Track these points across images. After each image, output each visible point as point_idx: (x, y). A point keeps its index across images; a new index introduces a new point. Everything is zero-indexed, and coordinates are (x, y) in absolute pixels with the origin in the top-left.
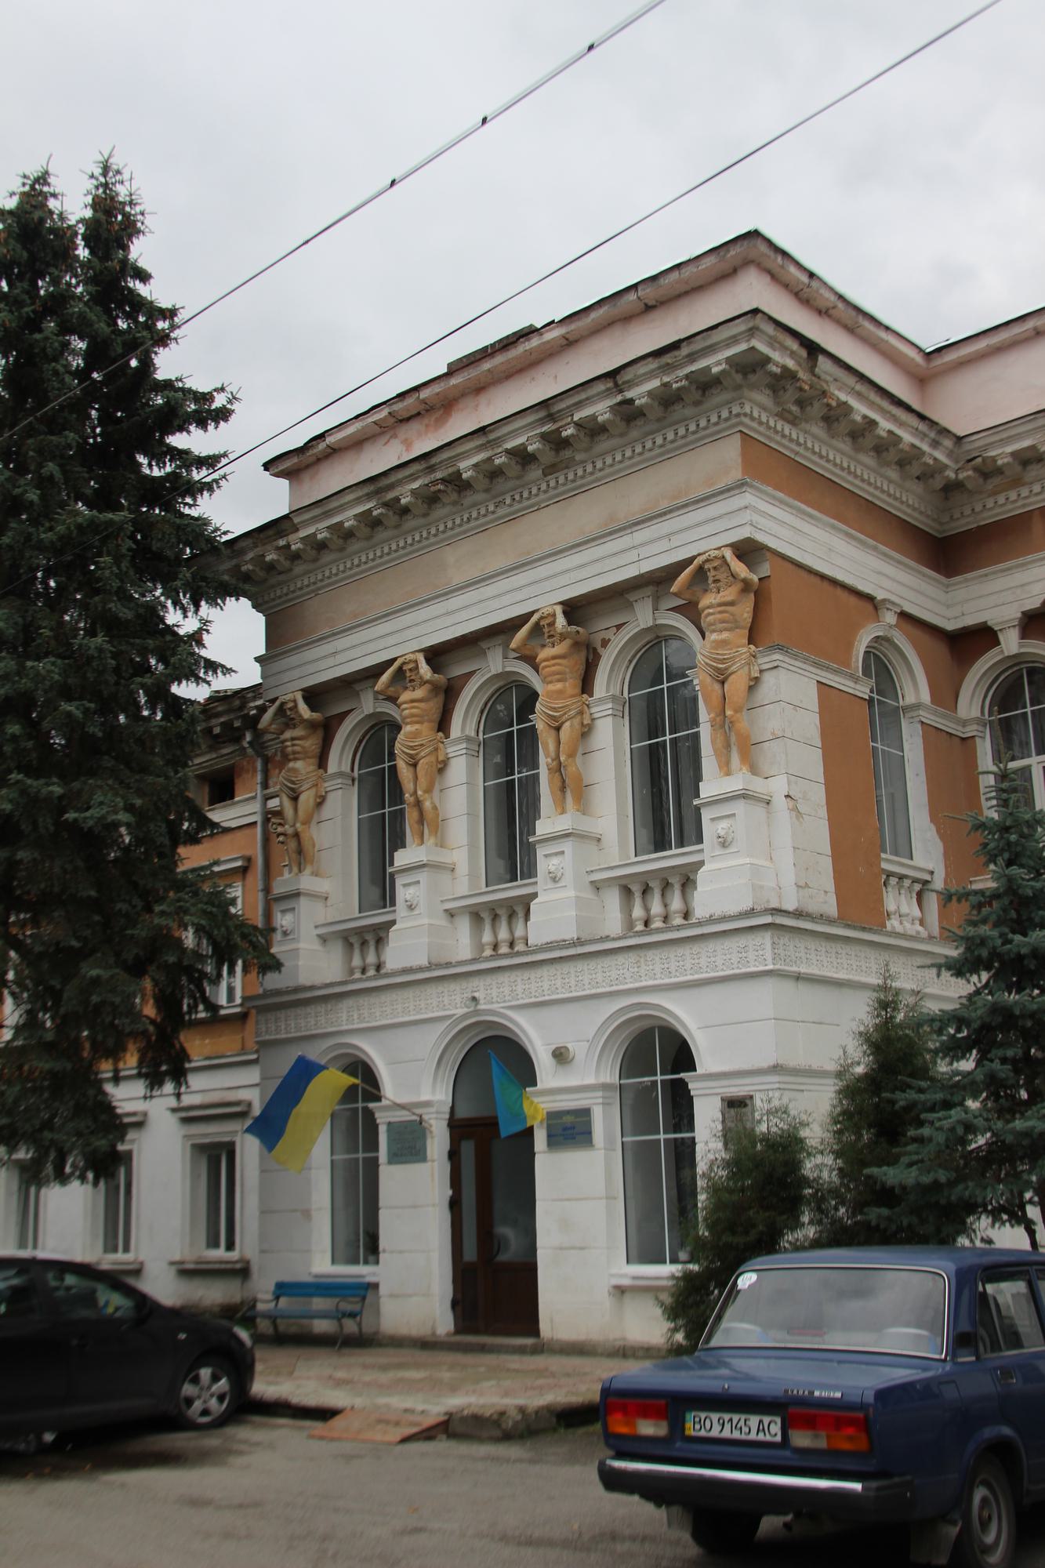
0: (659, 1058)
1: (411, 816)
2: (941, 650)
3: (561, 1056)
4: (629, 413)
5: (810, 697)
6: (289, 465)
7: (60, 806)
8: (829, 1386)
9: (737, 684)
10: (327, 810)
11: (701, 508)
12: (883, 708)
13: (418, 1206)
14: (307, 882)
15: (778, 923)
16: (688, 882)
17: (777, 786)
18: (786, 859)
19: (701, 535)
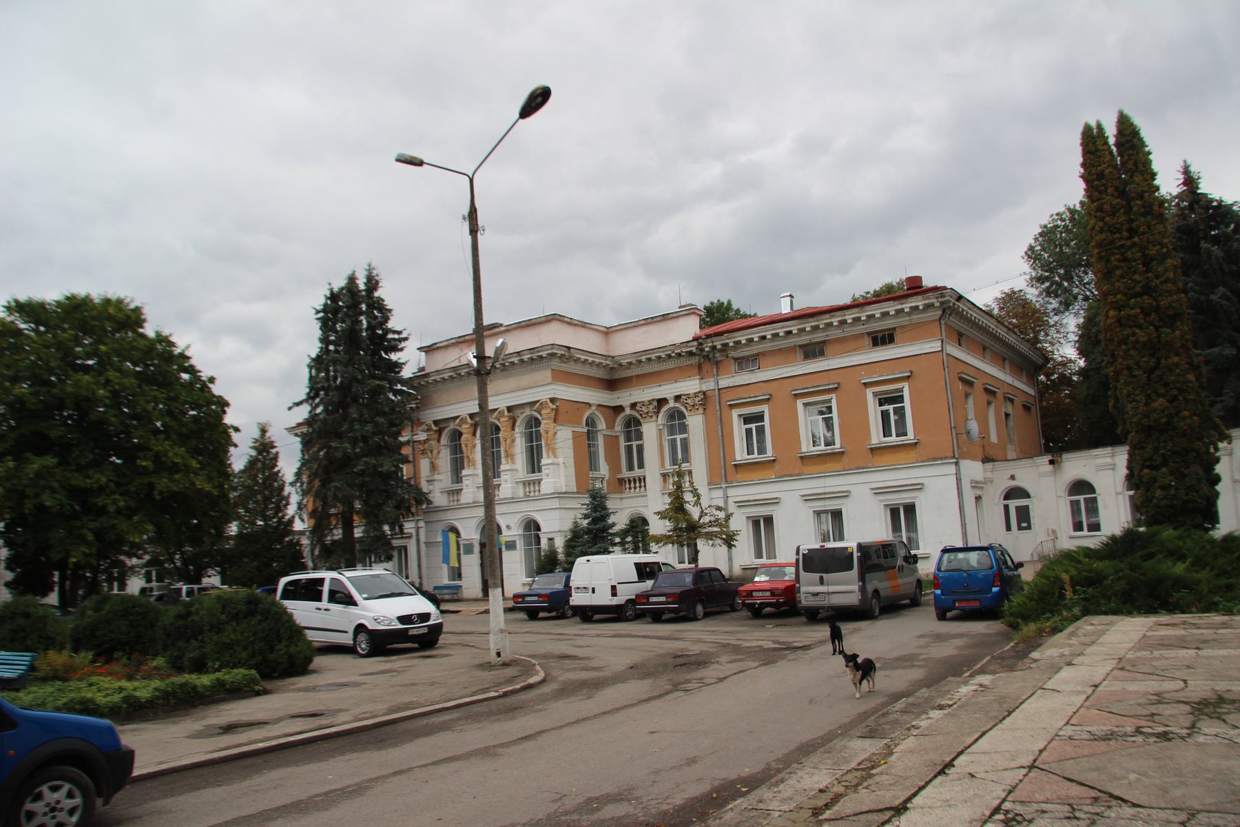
0: (532, 527)
1: (466, 460)
2: (611, 411)
3: (508, 527)
4: (522, 361)
5: (570, 435)
6: (428, 350)
7: (375, 466)
8: (543, 592)
9: (550, 434)
10: (441, 455)
11: (540, 388)
12: (591, 435)
13: (471, 566)
14: (437, 477)
15: (560, 495)
16: (539, 481)
17: (561, 460)
18: (563, 479)
19: (543, 394)
